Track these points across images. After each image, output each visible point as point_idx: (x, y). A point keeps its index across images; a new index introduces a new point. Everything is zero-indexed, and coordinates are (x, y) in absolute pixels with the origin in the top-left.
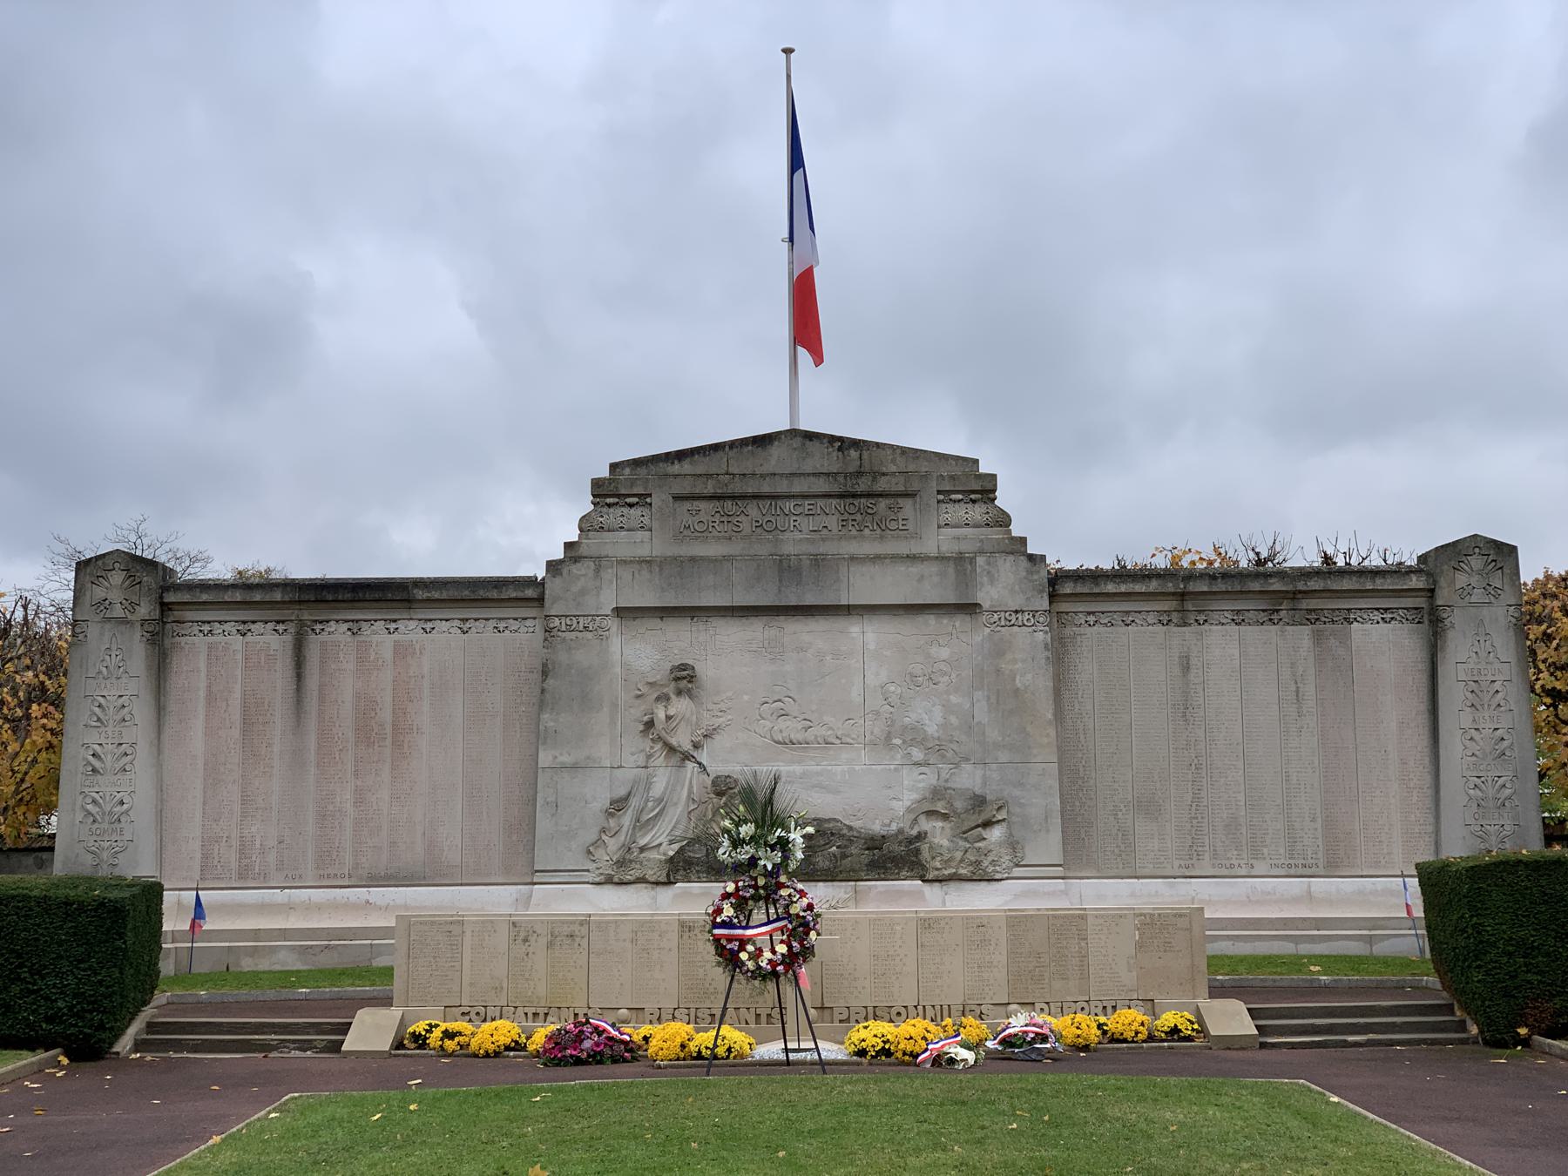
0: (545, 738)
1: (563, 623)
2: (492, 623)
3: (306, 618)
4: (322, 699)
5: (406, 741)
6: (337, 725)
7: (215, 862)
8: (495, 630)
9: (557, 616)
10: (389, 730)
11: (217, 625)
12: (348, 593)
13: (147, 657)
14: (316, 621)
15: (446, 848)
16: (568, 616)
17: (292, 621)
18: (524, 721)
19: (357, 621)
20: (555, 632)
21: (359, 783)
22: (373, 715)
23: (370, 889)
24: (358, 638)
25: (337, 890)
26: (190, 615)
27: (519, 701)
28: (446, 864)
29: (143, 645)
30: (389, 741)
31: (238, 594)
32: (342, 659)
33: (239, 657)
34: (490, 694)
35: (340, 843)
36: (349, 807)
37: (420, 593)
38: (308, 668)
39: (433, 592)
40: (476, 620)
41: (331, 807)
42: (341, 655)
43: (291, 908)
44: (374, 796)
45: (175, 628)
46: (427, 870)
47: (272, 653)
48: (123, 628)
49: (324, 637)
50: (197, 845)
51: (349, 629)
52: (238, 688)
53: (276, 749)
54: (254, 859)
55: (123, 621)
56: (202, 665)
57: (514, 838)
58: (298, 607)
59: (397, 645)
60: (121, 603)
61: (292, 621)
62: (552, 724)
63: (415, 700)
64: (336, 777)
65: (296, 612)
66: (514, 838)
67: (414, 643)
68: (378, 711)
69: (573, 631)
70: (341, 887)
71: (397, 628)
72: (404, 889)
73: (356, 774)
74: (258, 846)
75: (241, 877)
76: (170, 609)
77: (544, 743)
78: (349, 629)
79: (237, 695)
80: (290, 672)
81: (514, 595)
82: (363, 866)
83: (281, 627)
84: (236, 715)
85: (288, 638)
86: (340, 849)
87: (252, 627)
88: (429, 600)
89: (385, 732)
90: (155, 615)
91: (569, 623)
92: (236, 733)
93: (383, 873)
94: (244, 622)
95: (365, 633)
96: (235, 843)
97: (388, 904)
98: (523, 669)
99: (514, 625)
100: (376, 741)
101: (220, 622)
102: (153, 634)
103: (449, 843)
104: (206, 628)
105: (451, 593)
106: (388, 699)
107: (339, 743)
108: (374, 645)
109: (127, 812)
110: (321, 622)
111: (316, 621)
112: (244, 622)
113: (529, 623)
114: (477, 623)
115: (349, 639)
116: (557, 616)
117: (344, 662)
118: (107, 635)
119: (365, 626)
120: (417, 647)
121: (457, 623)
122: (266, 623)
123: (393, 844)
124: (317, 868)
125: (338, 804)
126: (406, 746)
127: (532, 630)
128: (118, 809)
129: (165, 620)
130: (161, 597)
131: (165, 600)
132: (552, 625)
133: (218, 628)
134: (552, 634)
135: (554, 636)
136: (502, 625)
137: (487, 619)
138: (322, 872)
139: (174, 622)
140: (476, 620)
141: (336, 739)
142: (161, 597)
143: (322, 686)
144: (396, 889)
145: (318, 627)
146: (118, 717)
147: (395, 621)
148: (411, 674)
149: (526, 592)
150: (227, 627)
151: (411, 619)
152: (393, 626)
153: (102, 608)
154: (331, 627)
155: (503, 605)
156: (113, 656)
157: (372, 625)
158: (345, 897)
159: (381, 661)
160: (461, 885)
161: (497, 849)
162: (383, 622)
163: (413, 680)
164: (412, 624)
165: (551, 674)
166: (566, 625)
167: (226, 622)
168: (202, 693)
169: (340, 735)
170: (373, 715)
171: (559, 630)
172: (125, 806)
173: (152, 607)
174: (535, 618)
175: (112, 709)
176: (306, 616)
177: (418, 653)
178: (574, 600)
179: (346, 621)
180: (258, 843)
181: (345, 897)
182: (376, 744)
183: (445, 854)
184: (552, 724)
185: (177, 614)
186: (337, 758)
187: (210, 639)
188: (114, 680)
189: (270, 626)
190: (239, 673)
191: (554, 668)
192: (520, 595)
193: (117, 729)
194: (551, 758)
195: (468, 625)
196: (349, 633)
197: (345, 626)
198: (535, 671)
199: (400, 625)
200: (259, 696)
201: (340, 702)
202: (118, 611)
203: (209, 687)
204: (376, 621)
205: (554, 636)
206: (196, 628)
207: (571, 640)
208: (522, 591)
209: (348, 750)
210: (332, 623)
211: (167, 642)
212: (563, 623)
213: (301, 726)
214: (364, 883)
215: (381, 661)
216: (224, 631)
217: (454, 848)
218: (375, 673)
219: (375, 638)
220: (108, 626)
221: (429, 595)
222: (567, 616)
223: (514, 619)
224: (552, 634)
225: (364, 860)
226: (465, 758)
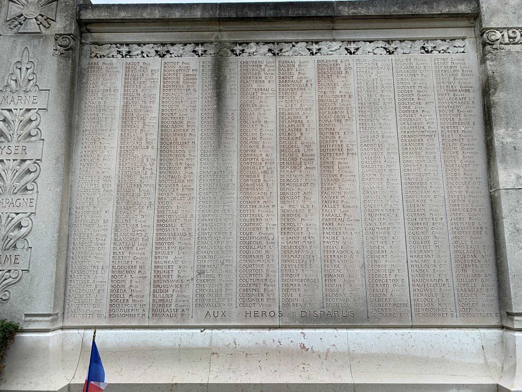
0: (504, 156)
1: (506, 35)
2: (418, 45)
3: (226, 39)
4: (243, 120)
5: (336, 162)
6: (261, 146)
7: (127, 297)
8: (423, 51)
9: (498, 29)
10: (316, 150)
11: (136, 46)
12: (271, 9)
13: (59, 69)
14: (235, 43)
15: (391, 284)
16: (512, 28)
17: (211, 43)
18: (465, 142)
19: (278, 43)
20: (497, 45)
21: (286, 207)
22: (298, 135)
23: (305, 331)
24: (278, 59)
25: (266, 332)
26: (107, 37)
27: (456, 120)
28: (392, 302)
29: (55, 58)
30: (316, 163)
31: (157, 12)
32: (263, 79)
33: (157, 76)
34: (424, 113)
35: (268, 275)
36: (276, 232)
37: (346, 9)
38: (228, 87)
39: (360, 9)
40: (402, 41)
41: (256, 234)
42: (263, 75)
43: (213, 353)
44: (304, 223)
45: (93, 49)
46: (370, 309)
47: (191, 72)
48: (36, 42)
49: (244, 57)
50: (107, 276)
51: (270, 50)
52: (156, 106)
53: (196, 170)
54: (170, 292)
55: (37, 35)
56: (119, 84)
57: (470, 272)
58: (218, 28)
59: (320, 65)
60: (36, 19)
61: (211, 43)
62: (509, 140)
63: (343, 120)
64: (261, 201)
65: (216, 33)
66: (470, 272)
67: (339, 62)
68: (303, 131)
69: (517, 43)
70: (270, 328)
71: (319, 49)
72: (344, 331)
73: (283, 198)
74: (175, 278)
75: (155, 314)
76: (89, 31)
77: (504, 161)
78: (270, 50)
79: (155, 113)
80: (210, 92)
81: (446, 10)
82: (295, 302)
83: (200, 49)
84: (154, 136)
85: (208, 59)
86: (268, 283)
87: (171, 49)
88: (355, 18)
89: (312, 153)
90: (71, 30)
91: (512, 35)
92: (152, 153)
93: (318, 312)
94: (163, 44)
95: (287, 54)
96: (149, 274)
97: (328, 350)
98: (458, 88)
99: (444, 46)
100: (303, 163)
101: (139, 45)
102: (68, 48)
103: (393, 277)
104: (124, 49)
105: (378, 9)
106: (314, 117)
107: (263, 164)
108: (296, 66)
109: (24, 237)
110: (240, 44)
111: (235, 43)
112: (163, 44)
113: (458, 43)
114: (403, 44)
115: (271, 60)
116: (498, 29)
117: (266, 81)
118: (19, 48)
119: (286, 47)
120: (343, 66)
121: (382, 44)
122: (185, 45)
123: (329, 277)
124: (243, 304)
125: (264, 230)
126: (336, 167)
127: (462, 50)
128: (17, 233)
129: (83, 41)
130: (78, 14)
131: (82, 17)
132: (493, 38)
133: (136, 50)
134: (494, 46)
135: (497, 49)
136: (429, 46)
137: (413, 40)
138: (248, 309)
139: (94, 43)
140: (402, 41)
141: (260, 159)
142: (78, 14)
143: (243, 106)
144: (335, 331)
145: (238, 49)
146: (25, 131)
147: (317, 43)
148: (338, 93)
149: (459, 8)
150: (145, 49)
151: (334, 40)
152: (315, 47)
153: (17, 23)
154: (251, 48)
155: (431, 24)
156: (24, 69)
157: (293, 46)
158: (276, 340)
159: (304, 81)
160: (412, 327)
161: (451, 284)
162: (304, 44)
163: (340, 99)
164: (335, 45)
165: (500, 86)
166: (510, 38)
167: (144, 44)
168: (118, 113)
169: (264, 156)
170: (298, 135)
171: (501, 43)
172: (23, 230)
173: (68, 22)
174: (463, 39)
175: (17, 124)
176: (225, 37)
177: (344, 72)
178: (513, 13)
179: (266, 43)
180: (175, 274)
181: (276, 340)
182: (303, 168)
183: (390, 290)
184: (509, 140)
185: (96, 36)
186: (262, 181)
187: (128, 60)
188: (22, 94)
189: (189, 48)
190: (157, 92)
191: (503, 81)
192: (453, 10)
193: (21, 144)
194: (513, 177)
195: (393, 45)
196: (270, 54)
197: (266, 47)
198: (471, 90)
199: (324, 46)
200: (178, 116)
201: (263, 123)
202: (32, 26)
203: (126, 105)
204: (297, 43)
205: (497, 49)
206: (114, 50)
207: (518, 52)
208: (454, 7)
209: (272, 172)
210: (252, 44)
211: (85, 62)
212: (506, 35)
213: (222, 147)
214: (297, 324)
215: (304, 81)
216: (142, 52)
217: (400, 282)
218: (299, 93)
219: (297, 59)
220: (21, 40)
221: (356, 11)
222: (508, 29)
223: (442, 40)
224: (494, 46)
225: (295, 295)
226: (403, 181)
